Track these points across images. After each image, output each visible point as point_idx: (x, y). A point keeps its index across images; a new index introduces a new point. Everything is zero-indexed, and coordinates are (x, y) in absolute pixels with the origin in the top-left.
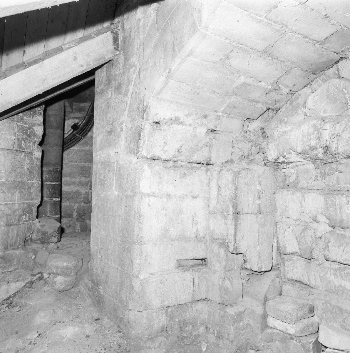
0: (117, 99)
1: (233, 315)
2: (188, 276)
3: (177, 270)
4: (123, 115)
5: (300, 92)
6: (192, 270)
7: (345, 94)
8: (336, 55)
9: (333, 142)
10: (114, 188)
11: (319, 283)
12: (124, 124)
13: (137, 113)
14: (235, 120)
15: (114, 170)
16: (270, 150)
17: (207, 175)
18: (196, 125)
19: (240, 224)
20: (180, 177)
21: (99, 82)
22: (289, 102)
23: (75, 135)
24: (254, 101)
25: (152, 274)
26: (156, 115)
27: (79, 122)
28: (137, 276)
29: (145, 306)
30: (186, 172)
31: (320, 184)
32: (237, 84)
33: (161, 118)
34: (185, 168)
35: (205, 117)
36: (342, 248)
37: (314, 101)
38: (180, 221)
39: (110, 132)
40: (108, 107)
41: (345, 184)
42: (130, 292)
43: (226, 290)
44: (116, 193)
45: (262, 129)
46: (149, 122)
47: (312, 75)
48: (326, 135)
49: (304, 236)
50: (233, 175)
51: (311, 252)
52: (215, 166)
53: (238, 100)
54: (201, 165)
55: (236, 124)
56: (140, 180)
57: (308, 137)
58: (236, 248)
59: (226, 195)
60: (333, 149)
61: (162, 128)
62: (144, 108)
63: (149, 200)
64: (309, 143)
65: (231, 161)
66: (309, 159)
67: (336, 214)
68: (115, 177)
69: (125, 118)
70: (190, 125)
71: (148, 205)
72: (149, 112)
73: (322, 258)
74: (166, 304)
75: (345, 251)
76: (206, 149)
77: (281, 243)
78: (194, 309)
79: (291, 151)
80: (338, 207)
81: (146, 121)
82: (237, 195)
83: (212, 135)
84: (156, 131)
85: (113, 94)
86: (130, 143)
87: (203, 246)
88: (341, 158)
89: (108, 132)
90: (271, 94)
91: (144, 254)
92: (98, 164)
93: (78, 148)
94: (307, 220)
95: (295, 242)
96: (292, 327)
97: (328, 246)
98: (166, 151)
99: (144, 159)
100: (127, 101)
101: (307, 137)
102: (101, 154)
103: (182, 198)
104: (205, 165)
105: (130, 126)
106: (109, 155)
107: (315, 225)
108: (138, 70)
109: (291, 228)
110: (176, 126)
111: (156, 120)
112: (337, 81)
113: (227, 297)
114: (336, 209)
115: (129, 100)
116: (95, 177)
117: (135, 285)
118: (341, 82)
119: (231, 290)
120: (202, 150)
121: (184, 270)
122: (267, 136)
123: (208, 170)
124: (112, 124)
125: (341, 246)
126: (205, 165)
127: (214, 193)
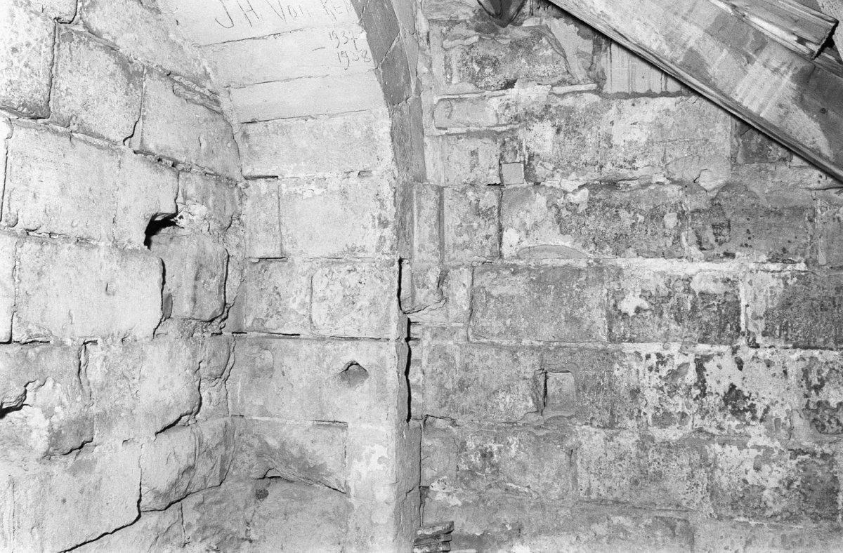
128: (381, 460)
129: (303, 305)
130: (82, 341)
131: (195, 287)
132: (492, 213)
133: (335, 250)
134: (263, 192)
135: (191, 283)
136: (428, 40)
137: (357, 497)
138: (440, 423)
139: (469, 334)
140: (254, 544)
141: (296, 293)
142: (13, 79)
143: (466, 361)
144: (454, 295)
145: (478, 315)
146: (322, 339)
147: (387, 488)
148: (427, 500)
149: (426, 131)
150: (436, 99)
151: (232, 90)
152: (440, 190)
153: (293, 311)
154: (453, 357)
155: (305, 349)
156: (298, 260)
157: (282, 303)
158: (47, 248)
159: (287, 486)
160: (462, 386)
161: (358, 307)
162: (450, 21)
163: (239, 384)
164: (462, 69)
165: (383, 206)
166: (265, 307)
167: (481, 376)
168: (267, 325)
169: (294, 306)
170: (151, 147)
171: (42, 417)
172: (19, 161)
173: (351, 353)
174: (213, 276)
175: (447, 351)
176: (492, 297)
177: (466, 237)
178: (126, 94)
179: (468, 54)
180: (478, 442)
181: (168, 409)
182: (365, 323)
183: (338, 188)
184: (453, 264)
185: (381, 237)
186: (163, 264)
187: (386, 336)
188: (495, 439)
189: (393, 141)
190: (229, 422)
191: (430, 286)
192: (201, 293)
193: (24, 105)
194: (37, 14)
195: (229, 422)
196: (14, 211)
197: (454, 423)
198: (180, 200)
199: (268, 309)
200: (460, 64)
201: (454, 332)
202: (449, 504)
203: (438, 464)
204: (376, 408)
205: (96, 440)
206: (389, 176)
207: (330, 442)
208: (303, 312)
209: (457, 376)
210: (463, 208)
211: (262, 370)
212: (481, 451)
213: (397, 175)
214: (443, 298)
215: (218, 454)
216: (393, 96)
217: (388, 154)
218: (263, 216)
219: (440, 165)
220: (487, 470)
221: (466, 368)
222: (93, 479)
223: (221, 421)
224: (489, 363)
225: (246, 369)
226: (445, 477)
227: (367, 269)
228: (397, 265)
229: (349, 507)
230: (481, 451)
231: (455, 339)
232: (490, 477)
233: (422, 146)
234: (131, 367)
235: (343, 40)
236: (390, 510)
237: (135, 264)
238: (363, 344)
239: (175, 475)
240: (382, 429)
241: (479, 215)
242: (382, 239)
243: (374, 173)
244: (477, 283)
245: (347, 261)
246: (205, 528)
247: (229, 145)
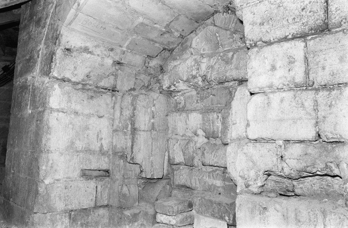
0: (37, 31)
1: (129, 215)
2: (92, 184)
3: (81, 178)
4: (40, 44)
5: (188, 37)
6: (95, 179)
7: (217, 37)
8: (210, 8)
9: (208, 72)
10: (28, 107)
11: (198, 186)
12: (41, 52)
13: (51, 41)
14: (138, 56)
15: (30, 92)
16: (164, 81)
17: (112, 100)
18: (104, 56)
19: (137, 138)
20: (88, 99)
21: (23, 19)
22: (180, 44)
23: (6, 76)
24: (152, 41)
25: (58, 180)
26: (67, 43)
27: (10, 65)
28: (42, 180)
29: (49, 208)
30: (94, 95)
31: (200, 105)
32: (136, 23)
33: (71, 46)
34: (93, 91)
35: (112, 50)
36: (213, 153)
38: (86, 136)
39: (29, 60)
40: (29, 39)
41: (217, 104)
42: (36, 196)
43: (124, 195)
44: (30, 112)
45: (161, 66)
46: (61, 48)
47: (196, 23)
48: (204, 67)
49: (188, 148)
50: (132, 97)
51: (193, 160)
52: (119, 92)
53: (139, 38)
54: (107, 91)
55: (138, 60)
56: (50, 97)
58: (132, 159)
59: (126, 115)
61: (73, 55)
62: (57, 36)
63: (58, 115)
64: (191, 73)
65: (134, 89)
66: (193, 87)
67: (210, 128)
68: (30, 98)
69: (42, 46)
70: (98, 55)
71: (57, 119)
72: (61, 39)
73: (200, 164)
74: (70, 207)
75: (215, 155)
76: (112, 78)
77: (171, 156)
78: (97, 214)
79: (179, 80)
81: (58, 47)
82: (135, 114)
83: (117, 67)
84: (67, 56)
85: (34, 28)
86: (44, 66)
87: (106, 159)
88: (215, 85)
89: (27, 60)
90: (166, 36)
91: (51, 162)
92: (17, 89)
93: (8, 88)
94: (190, 135)
95: (181, 153)
96: (174, 219)
97: (204, 153)
98: (76, 75)
99: (55, 80)
100: (44, 32)
101: (190, 69)
102: (21, 80)
103: (89, 116)
104: (111, 91)
105: (45, 52)
106: (27, 80)
107: (196, 138)
108: (54, 5)
110: (85, 54)
111: (67, 47)
112: (212, 27)
113: (124, 201)
115: (46, 31)
116: (13, 101)
117: (40, 189)
118: (215, 28)
119: (128, 195)
120: (109, 77)
121: (87, 179)
122: (164, 72)
123: (113, 96)
124: (31, 53)
126: (111, 91)
127: (118, 113)
142: (304, 21)
158: (334, 93)
172: (312, 56)
193: (312, 29)
196: (311, 79)
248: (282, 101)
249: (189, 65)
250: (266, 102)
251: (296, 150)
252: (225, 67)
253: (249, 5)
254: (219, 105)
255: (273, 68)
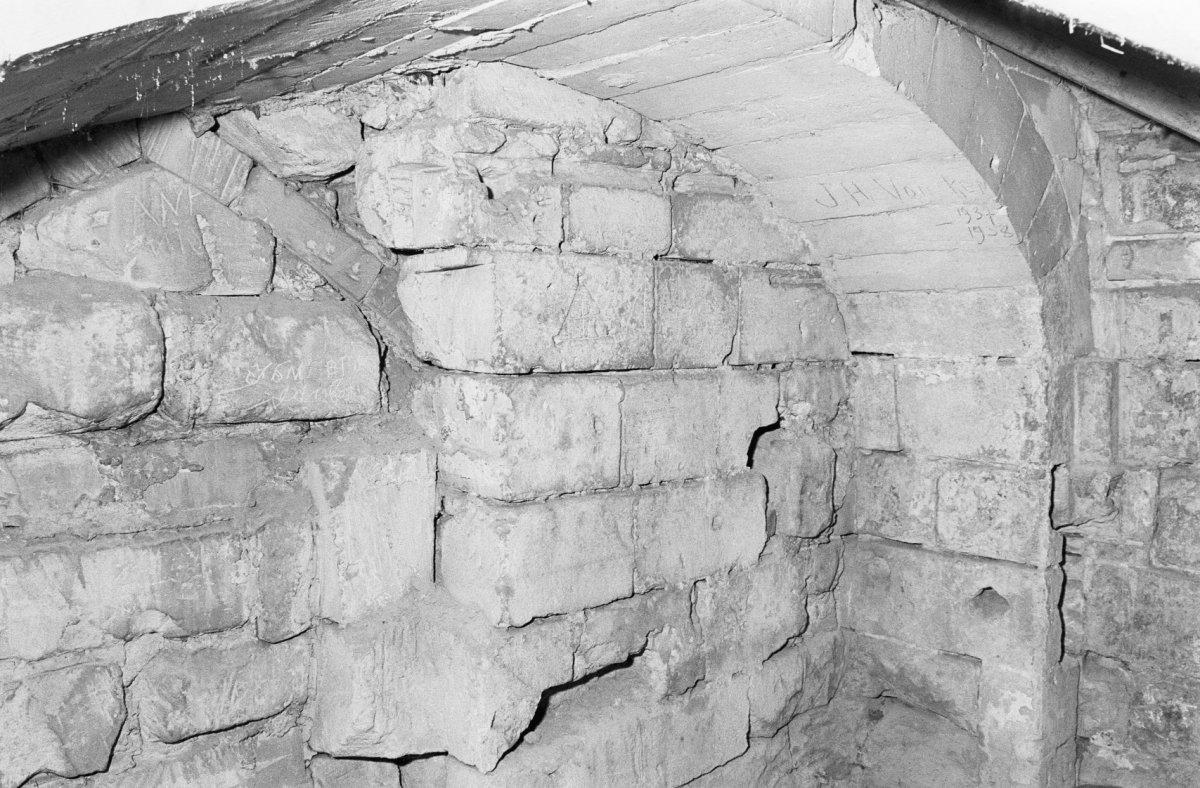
31: (123, 514)
37: (94, 225)
41: (210, 503)
49: (86, 699)
57: (120, 363)
60: (188, 402)
64: (124, 383)
67: (202, 597)
75: (235, 691)
80: (207, 575)
97: (185, 698)
101: (114, 361)
109: (22, 695)
114: (201, 581)
125: (225, 684)
128: (1023, 710)
129: (927, 513)
130: (693, 582)
131: (801, 502)
132: (1191, 401)
133: (968, 450)
134: (876, 373)
135: (796, 498)
136: (1097, 159)
137: (992, 746)
138: (1110, 663)
139: (1152, 556)
140: (866, 771)
141: (918, 497)
143: (1146, 592)
144: (1130, 504)
145: (1165, 534)
146: (950, 554)
147: (1031, 744)
148: (1085, 755)
149: (1095, 285)
150: (1109, 240)
151: (836, 262)
152: (1113, 368)
153: (914, 518)
154: (1128, 585)
155: (929, 565)
156: (920, 457)
157: (901, 506)
158: (659, 498)
159: (907, 712)
160: (1139, 622)
161: (997, 524)
162: (1131, 135)
163: (849, 594)
164: (1149, 202)
165: (1030, 403)
166: (880, 508)
167: (1167, 614)
168: (882, 530)
169: (916, 512)
170: (751, 358)
171: (660, 662)
173: (986, 578)
174: (819, 485)
175: (1119, 575)
176: (1187, 513)
177: (1150, 430)
178: (723, 309)
179: (1158, 181)
180: (1160, 697)
181: (774, 636)
182: (1009, 545)
183: (971, 376)
184: (1132, 463)
185: (1027, 442)
186: (766, 482)
187: (1033, 563)
188: (1185, 697)
189: (1044, 322)
190: (839, 637)
191: (1095, 495)
192: (808, 506)
193: (632, 363)
194: (637, 262)
195: (839, 637)
197: (1125, 665)
198: (782, 403)
199: (883, 512)
200: (1146, 196)
201: (1129, 552)
202: (1115, 765)
203: (1103, 715)
204: (1018, 649)
205: (708, 677)
206: (1039, 366)
207: (960, 677)
208: (924, 521)
209: (1132, 609)
210: (1148, 390)
211: (876, 578)
212: (1164, 708)
213: (1049, 361)
214: (1115, 509)
215: (826, 674)
216: (1043, 265)
217: (1038, 340)
218: (876, 400)
219: (1114, 330)
220: (1172, 734)
221: (1146, 600)
222: (705, 715)
223: (830, 636)
224: (1180, 598)
225: (857, 577)
226: (1111, 731)
227: (1008, 478)
228: (1048, 476)
229: (983, 757)
230: (1164, 708)
231: (1131, 561)
232: (1176, 744)
233: (1087, 310)
234: (738, 599)
235: (975, 216)
236: (1035, 770)
237: (739, 490)
238: (1004, 570)
239: (782, 704)
240: (1024, 674)
241: (1171, 401)
242: (1029, 445)
243: (1018, 360)
244: (1165, 492)
245: (981, 466)
246: (813, 752)
247: (833, 321)
248: (580, 522)
249: (111, 342)
250: (550, 525)
251: (604, 623)
252: (269, 369)
253: (509, 247)
254: (220, 506)
255: (565, 442)
